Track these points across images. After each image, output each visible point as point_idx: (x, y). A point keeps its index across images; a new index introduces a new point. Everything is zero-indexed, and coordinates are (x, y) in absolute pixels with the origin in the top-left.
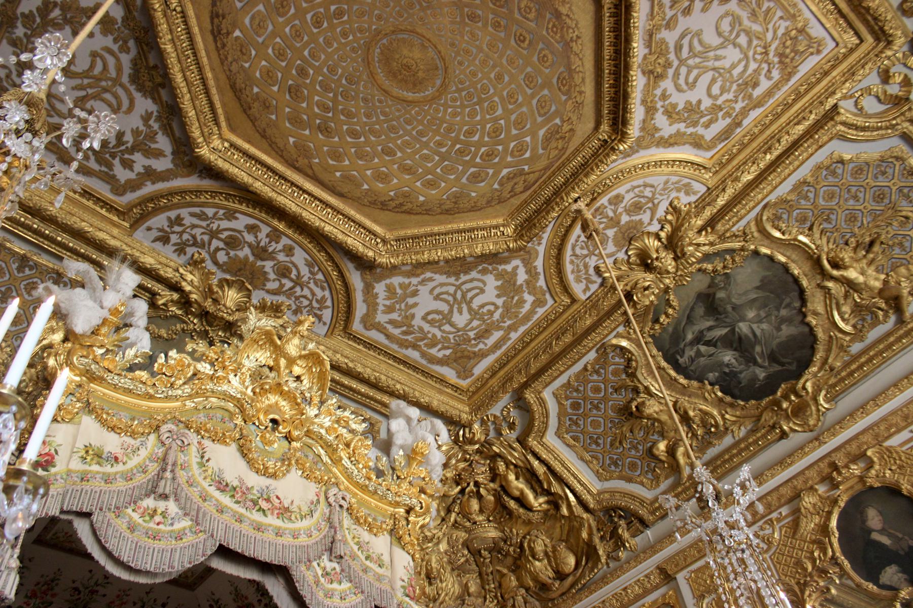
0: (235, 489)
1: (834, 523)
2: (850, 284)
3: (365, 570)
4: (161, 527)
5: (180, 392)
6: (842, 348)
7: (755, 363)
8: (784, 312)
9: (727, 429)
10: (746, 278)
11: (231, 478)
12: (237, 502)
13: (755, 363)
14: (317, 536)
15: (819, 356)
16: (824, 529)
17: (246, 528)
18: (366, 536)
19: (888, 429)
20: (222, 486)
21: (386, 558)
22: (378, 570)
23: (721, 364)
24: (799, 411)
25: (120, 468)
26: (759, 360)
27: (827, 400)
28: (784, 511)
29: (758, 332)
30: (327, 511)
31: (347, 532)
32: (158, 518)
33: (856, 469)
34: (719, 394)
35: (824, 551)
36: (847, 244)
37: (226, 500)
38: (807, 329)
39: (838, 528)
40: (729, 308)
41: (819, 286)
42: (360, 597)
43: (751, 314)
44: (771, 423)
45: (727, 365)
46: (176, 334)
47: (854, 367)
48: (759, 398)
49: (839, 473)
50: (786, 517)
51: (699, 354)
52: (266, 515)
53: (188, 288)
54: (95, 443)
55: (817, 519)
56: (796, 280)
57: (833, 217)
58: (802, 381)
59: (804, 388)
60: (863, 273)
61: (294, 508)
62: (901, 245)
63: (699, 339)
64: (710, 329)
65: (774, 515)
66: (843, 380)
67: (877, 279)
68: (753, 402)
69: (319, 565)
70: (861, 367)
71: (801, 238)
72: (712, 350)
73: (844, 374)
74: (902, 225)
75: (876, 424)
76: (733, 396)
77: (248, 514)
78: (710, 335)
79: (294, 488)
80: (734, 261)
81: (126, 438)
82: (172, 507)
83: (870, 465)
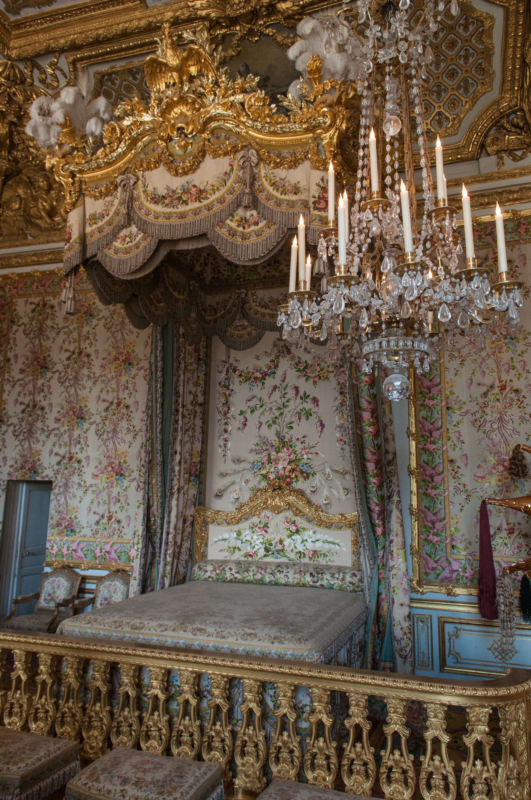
0: (164, 197)
3: (279, 203)
4: (130, 244)
5: (120, 150)
11: (162, 191)
12: (167, 205)
14: (229, 198)
17: (174, 221)
18: (281, 173)
20: (156, 199)
21: (302, 184)
22: (294, 198)
25: (107, 219)
30: (240, 173)
31: (264, 179)
32: (128, 239)
37: (159, 208)
42: (274, 227)
46: (238, 47)
52: (187, 204)
53: (204, 13)
54: (92, 212)
61: (209, 188)
69: (231, 221)
77: (175, 210)
79: (211, 171)
81: (107, 199)
82: (134, 229)
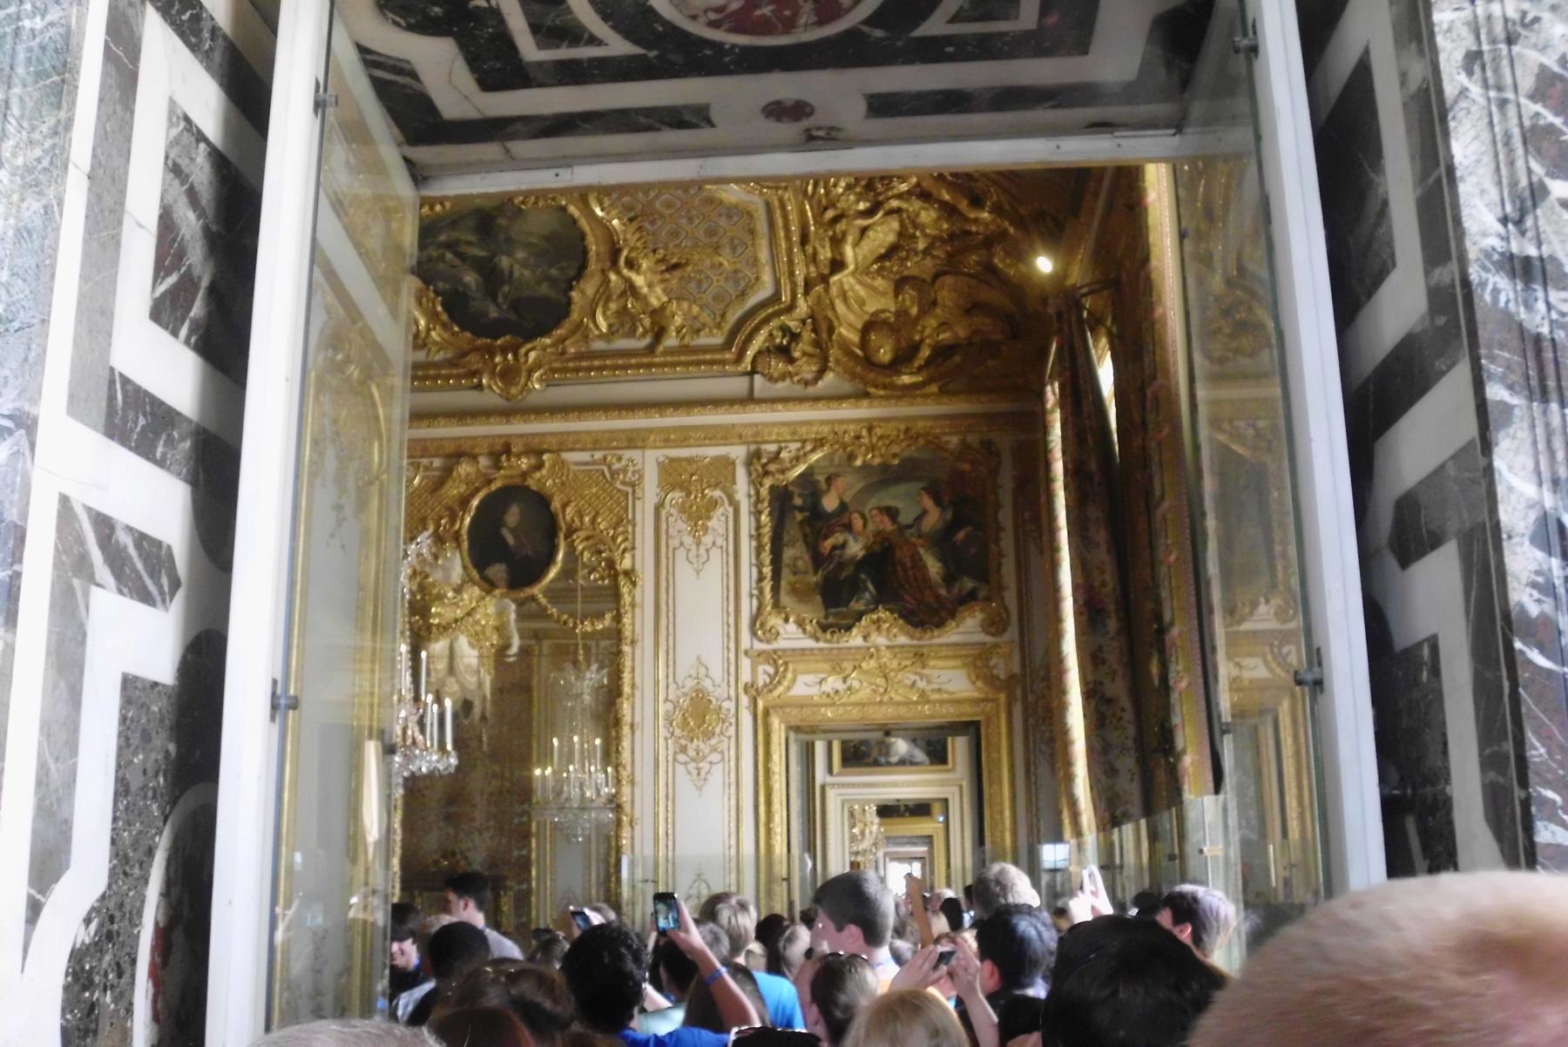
1: (475, 502)
2: (632, 289)
6: (586, 338)
7: (494, 298)
8: (554, 272)
9: (425, 345)
10: (538, 224)
13: (494, 298)
15: (560, 332)
16: (464, 502)
19: (575, 443)
23: (459, 280)
24: (508, 375)
26: (500, 300)
27: (540, 380)
28: (437, 463)
29: (516, 274)
33: (524, 463)
34: (439, 308)
35: (452, 523)
36: (654, 251)
38: (564, 301)
39: (478, 508)
40: (502, 237)
41: (603, 271)
43: (520, 255)
44: (475, 367)
45: (465, 285)
47: (584, 364)
48: (477, 333)
49: (508, 459)
50: (436, 469)
51: (442, 258)
55: (463, 488)
56: (585, 252)
57: (659, 223)
58: (529, 346)
59: (526, 355)
60: (650, 285)
62: (700, 282)
63: (450, 246)
64: (470, 243)
65: (425, 461)
66: (566, 370)
67: (658, 299)
68: (468, 334)
70: (590, 369)
71: (615, 222)
72: (457, 262)
73: (571, 365)
74: (713, 266)
75: (569, 433)
76: (451, 316)
78: (463, 249)
80: (536, 203)
83: (540, 466)
